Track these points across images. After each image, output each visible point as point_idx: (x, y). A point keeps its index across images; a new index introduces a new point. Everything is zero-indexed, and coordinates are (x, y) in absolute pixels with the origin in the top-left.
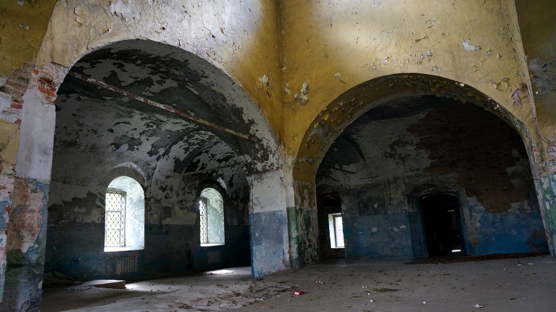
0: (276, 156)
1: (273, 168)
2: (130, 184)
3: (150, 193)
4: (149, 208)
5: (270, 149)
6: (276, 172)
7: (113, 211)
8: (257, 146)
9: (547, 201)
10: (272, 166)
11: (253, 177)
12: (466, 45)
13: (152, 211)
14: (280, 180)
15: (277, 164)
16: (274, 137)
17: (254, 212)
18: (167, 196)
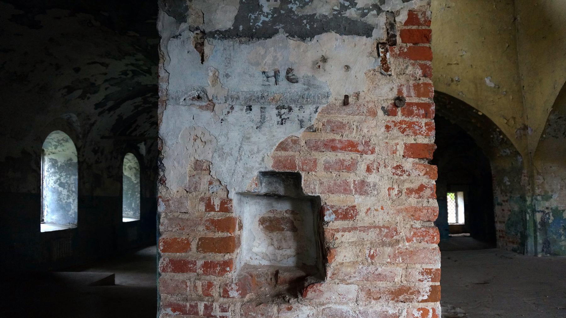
9: (528, 213)
12: (487, 81)
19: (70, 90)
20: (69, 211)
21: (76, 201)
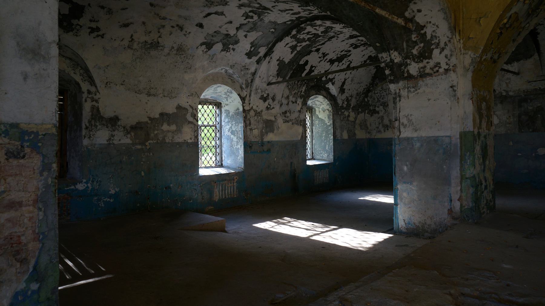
0: (447, 52)
1: (438, 71)
2: (226, 94)
3: (250, 104)
4: (248, 122)
5: (437, 41)
6: (444, 77)
7: (207, 126)
8: (414, 37)
10: (437, 68)
11: (401, 84)
13: (252, 126)
14: (451, 89)
15: (447, 64)
16: (448, 21)
17: (403, 135)
18: (269, 106)
19: (209, 46)
20: (238, 156)
21: (243, 146)
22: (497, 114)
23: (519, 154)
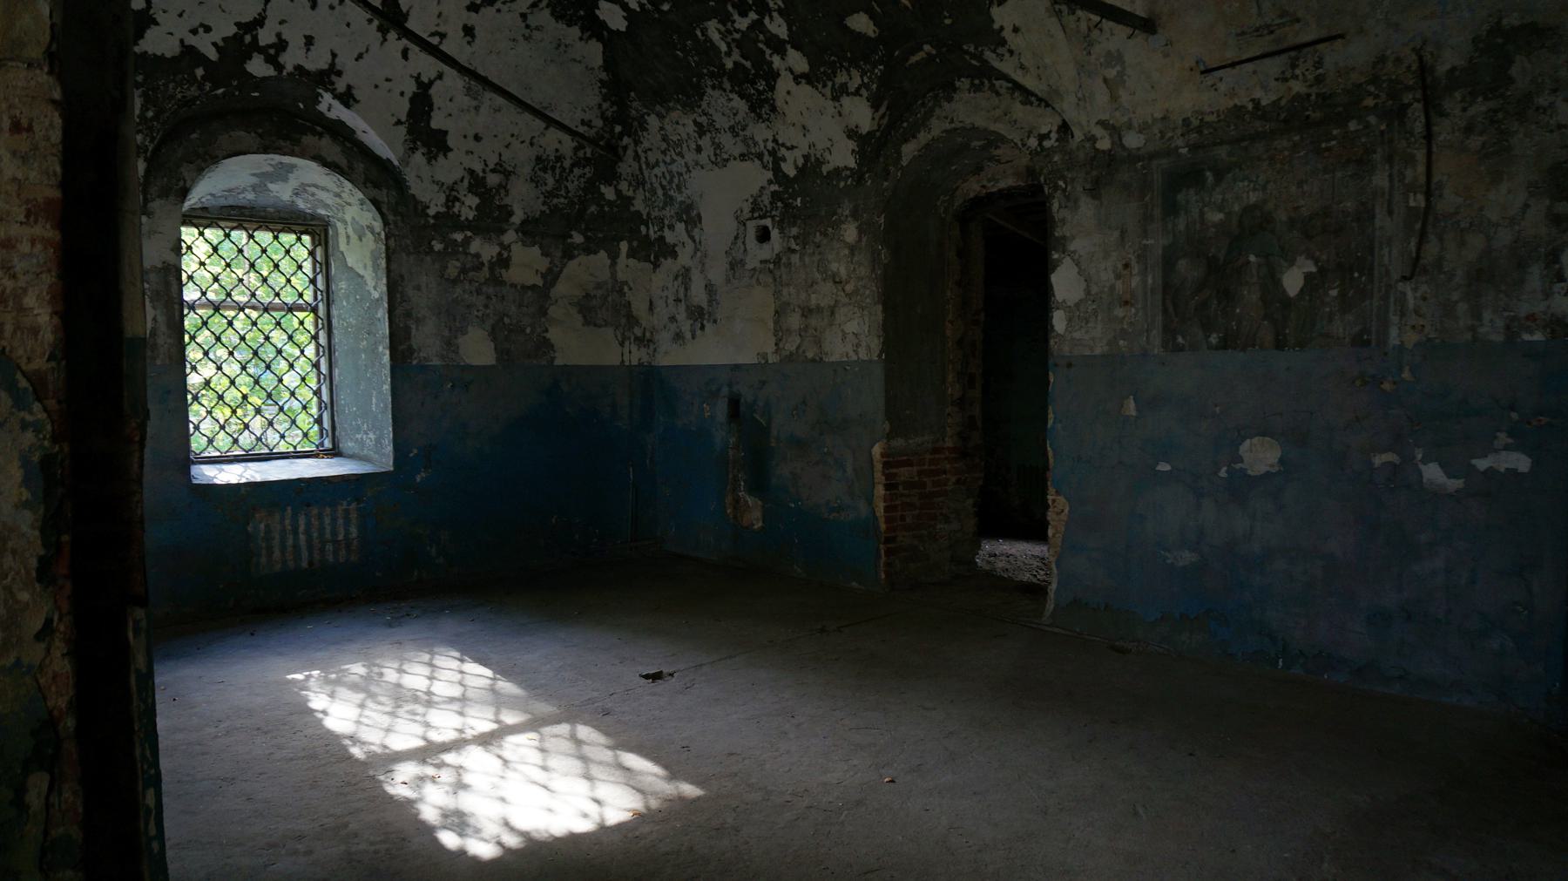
22: (1074, 252)
23: (1164, 467)
